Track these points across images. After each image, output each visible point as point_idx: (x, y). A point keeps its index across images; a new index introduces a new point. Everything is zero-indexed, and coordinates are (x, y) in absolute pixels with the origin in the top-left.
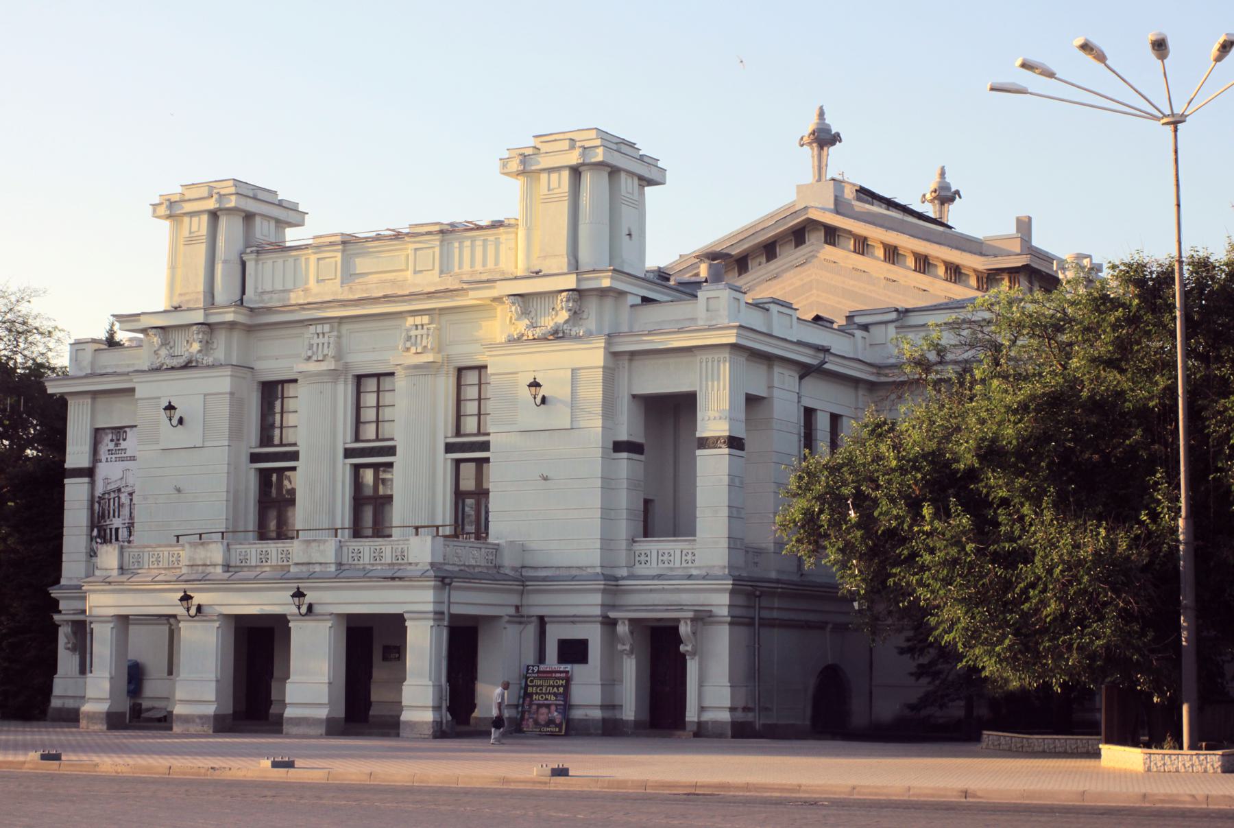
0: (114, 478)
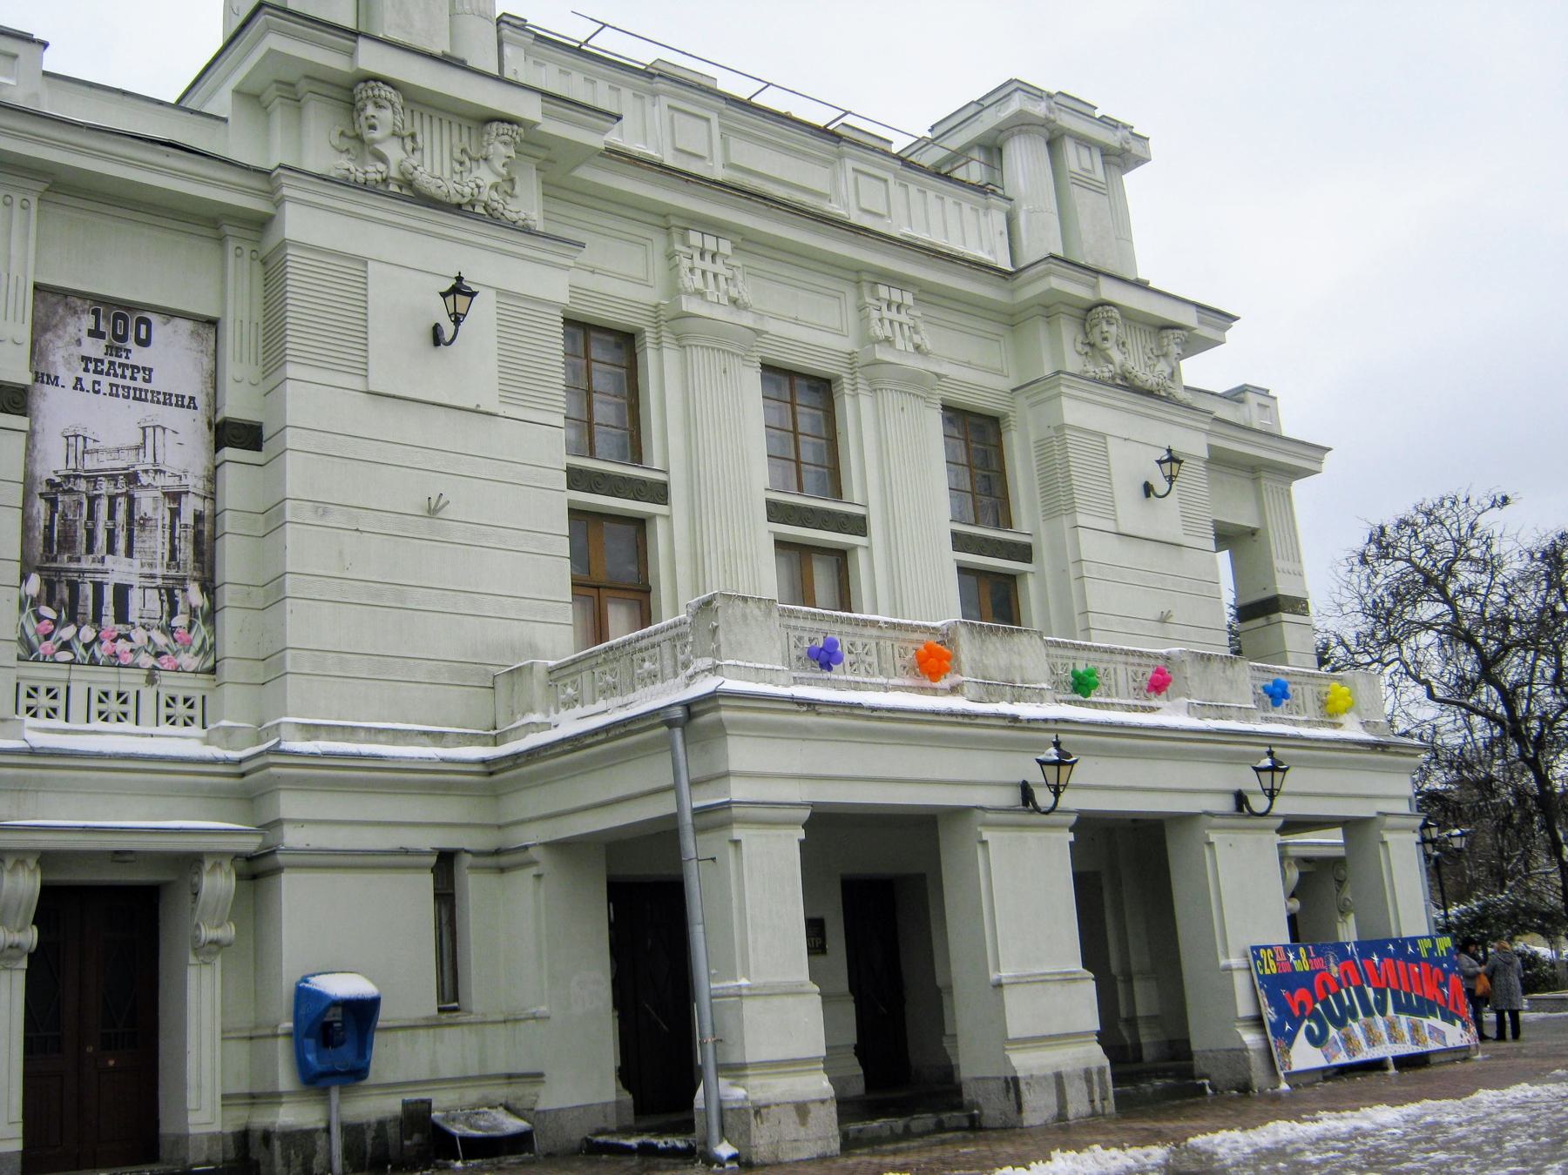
0: (107, 442)
